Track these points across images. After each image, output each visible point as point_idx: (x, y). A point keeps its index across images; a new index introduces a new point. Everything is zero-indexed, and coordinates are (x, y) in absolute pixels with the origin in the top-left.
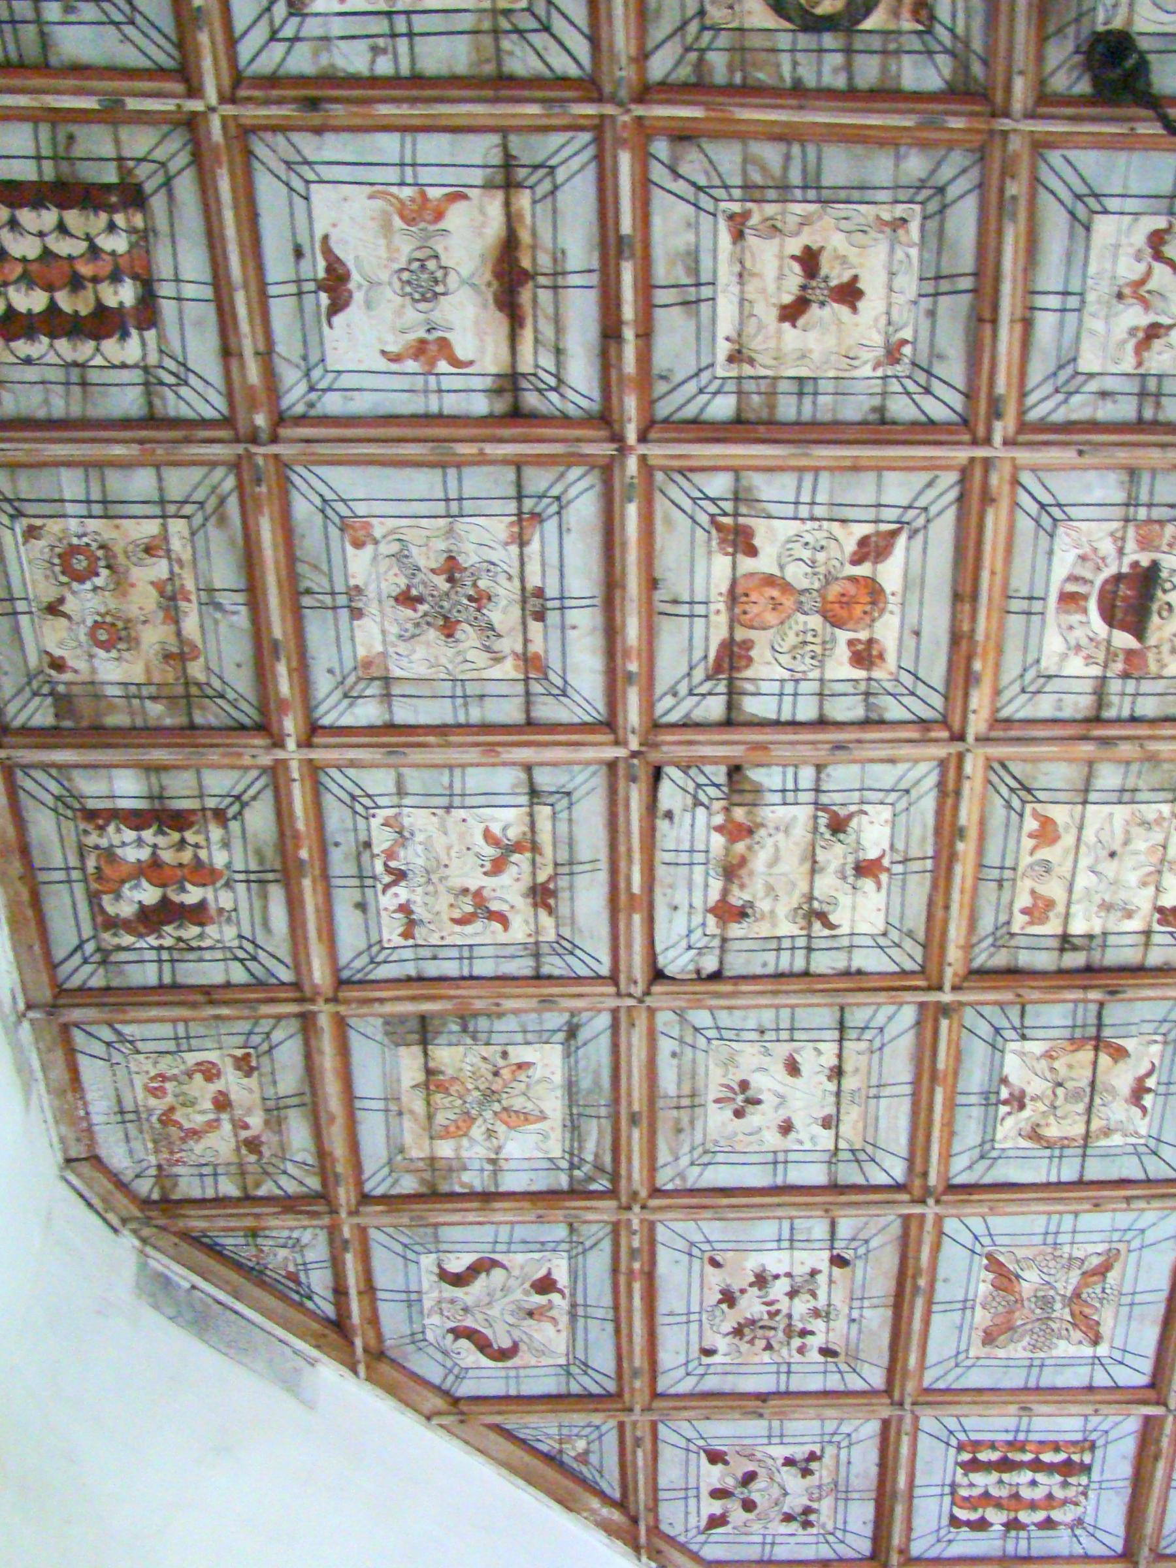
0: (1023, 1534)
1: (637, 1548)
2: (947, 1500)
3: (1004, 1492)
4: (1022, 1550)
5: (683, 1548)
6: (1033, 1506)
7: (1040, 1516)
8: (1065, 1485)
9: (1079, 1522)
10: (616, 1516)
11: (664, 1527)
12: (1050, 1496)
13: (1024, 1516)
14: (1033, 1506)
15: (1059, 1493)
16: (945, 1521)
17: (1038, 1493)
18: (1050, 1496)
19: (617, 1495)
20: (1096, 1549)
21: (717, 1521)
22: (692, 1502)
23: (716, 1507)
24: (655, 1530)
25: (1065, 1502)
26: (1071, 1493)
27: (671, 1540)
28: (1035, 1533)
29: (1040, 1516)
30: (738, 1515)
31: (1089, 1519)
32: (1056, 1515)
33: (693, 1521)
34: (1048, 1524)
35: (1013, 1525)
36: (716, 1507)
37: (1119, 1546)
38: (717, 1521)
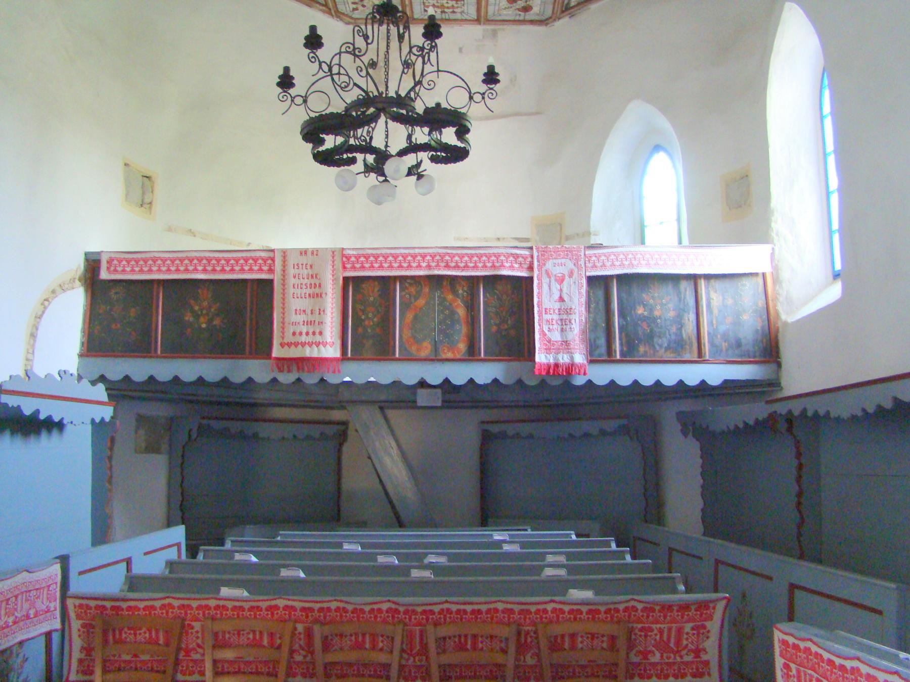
0: (447, 14)
1: (333, 16)
2: (422, 6)
3: (439, 5)
4: (447, 18)
5: (347, 15)
6: (448, 8)
7: (451, 10)
8: (457, 3)
9: (463, 12)
10: (324, 8)
11: (340, 10)
12: (453, 6)
13: (446, 10)
14: (448, 8)
15: (455, 5)
16: (423, 10)
17: (450, 5)
18: (453, 6)
19: (324, 3)
20: (468, 18)
21: (354, 9)
22: (347, 6)
23: (355, 6)
24: (337, 11)
25: (458, 7)
26: (460, 5)
27: (343, 14)
28: (450, 14)
29: (451, 10)
30: (361, 8)
31: (466, 11)
32: (455, 10)
33: (348, 9)
34: (454, 12)
35: (443, 12)
36: (355, 6)
37: (476, 18)
38: (354, 9)
